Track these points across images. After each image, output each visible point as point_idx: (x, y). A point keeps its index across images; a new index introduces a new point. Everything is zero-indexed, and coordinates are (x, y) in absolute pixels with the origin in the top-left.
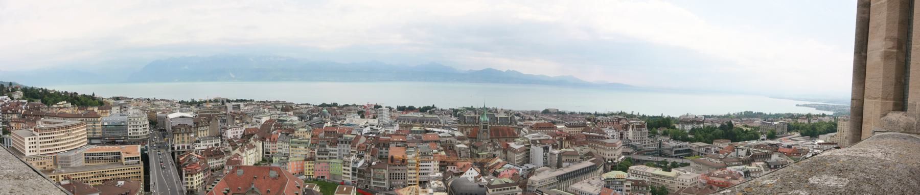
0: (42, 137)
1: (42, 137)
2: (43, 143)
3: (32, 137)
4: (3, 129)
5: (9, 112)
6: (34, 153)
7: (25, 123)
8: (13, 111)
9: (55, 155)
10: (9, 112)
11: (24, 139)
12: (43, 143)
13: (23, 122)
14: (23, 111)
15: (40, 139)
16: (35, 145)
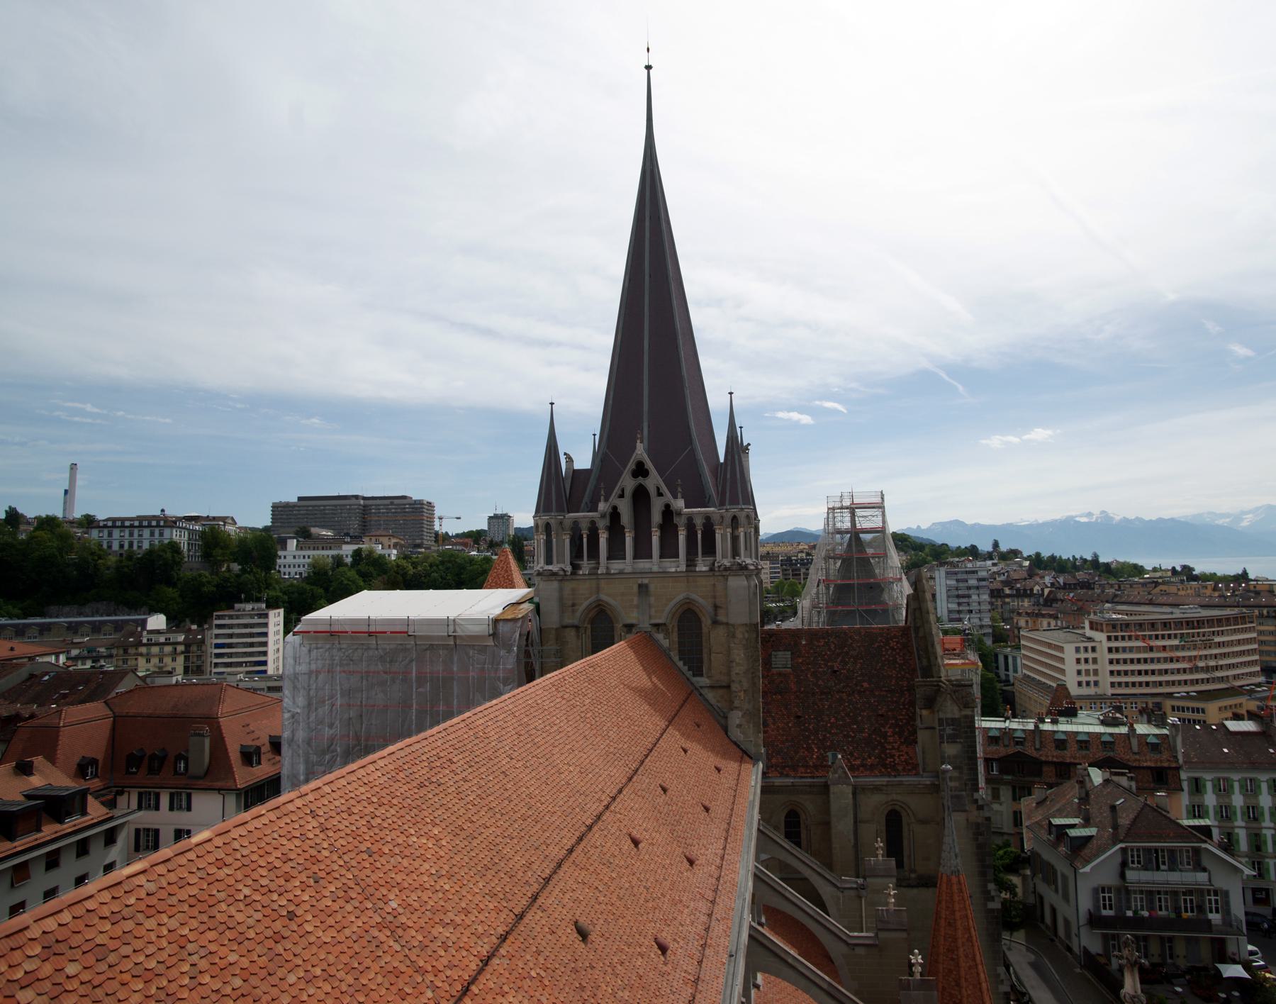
0: (1114, 644)
1: (1114, 644)
2: (1118, 661)
3: (1086, 644)
4: (994, 631)
5: (1007, 591)
6: (1091, 691)
7: (1056, 618)
8: (1018, 590)
9: (1158, 700)
10: (1007, 591)
11: (1061, 649)
12: (1119, 673)
13: (1051, 616)
14: (1046, 591)
15: (1111, 662)
16: (1094, 655)
